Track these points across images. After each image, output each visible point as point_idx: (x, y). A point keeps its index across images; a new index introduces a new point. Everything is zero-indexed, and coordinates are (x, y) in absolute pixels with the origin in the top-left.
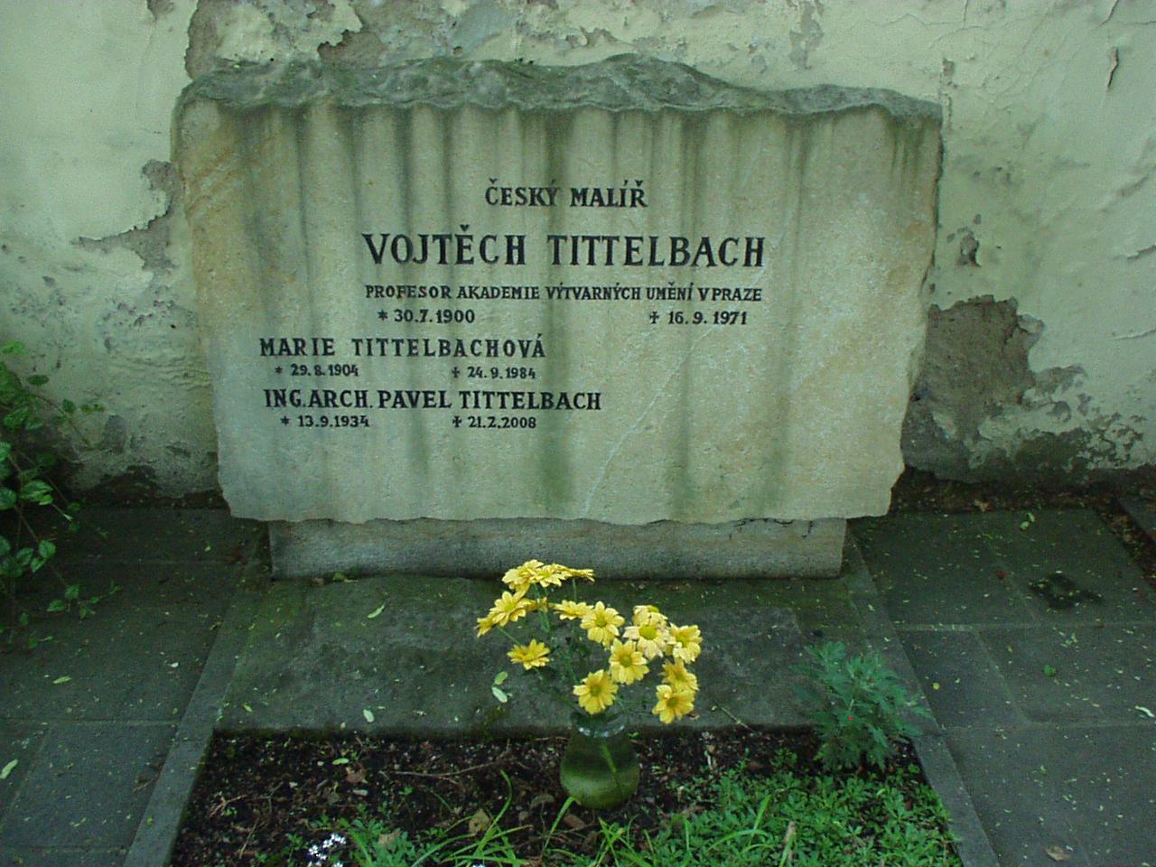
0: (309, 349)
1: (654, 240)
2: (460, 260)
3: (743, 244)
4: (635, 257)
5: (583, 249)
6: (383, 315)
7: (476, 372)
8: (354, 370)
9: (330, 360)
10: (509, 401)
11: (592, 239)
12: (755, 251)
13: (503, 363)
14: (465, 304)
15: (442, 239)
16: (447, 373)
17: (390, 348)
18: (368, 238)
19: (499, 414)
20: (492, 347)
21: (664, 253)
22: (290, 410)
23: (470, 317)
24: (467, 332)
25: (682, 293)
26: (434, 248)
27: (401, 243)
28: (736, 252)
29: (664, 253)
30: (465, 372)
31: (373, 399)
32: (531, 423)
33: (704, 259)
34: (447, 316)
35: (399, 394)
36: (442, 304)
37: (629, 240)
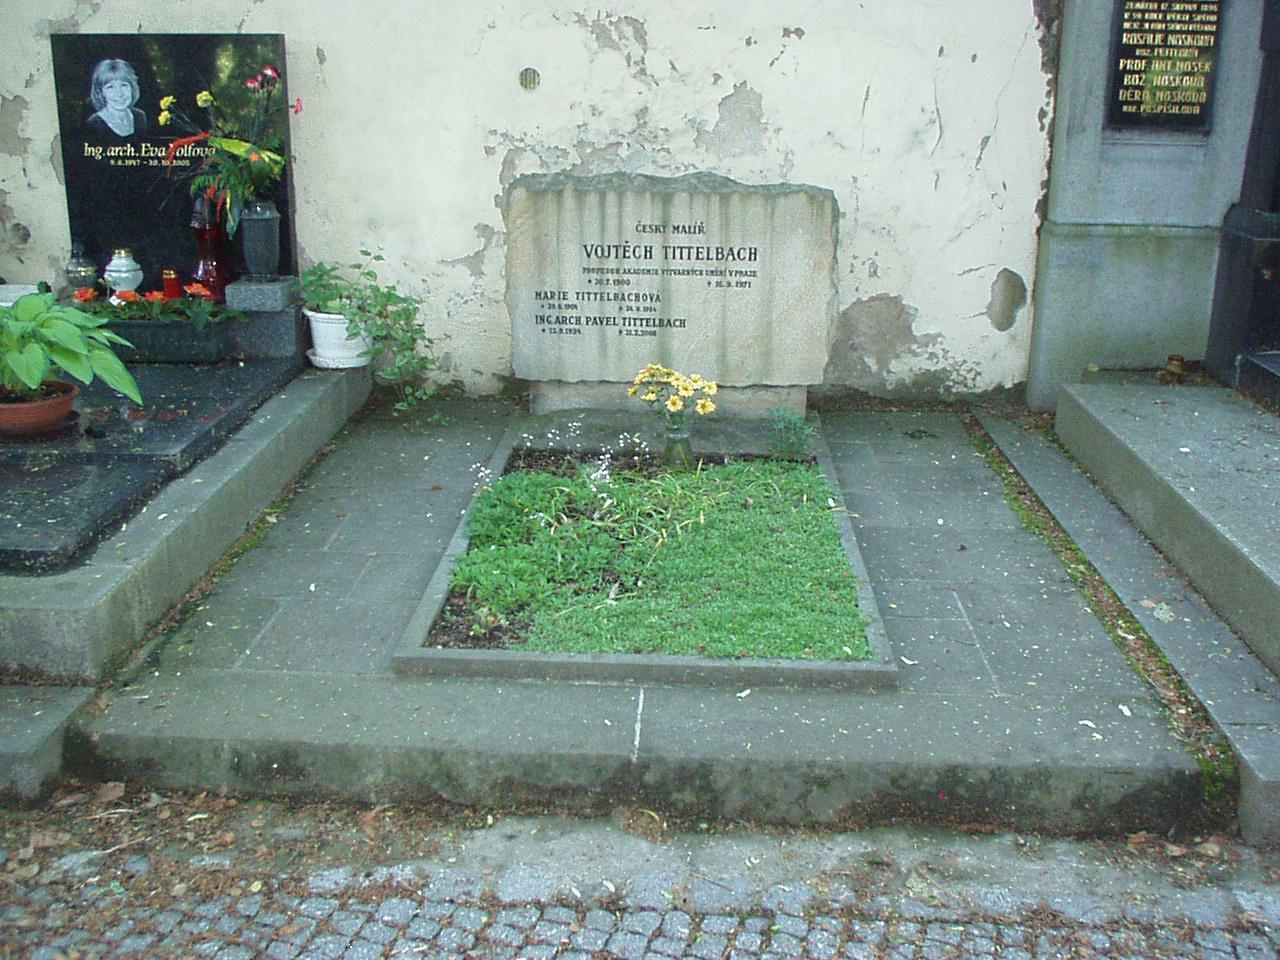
4: (701, 256)
5: (678, 252)
7: (630, 309)
8: (575, 306)
10: (644, 322)
11: (681, 248)
12: (753, 254)
13: (641, 304)
15: (616, 247)
16: (617, 309)
17: (592, 296)
18: (585, 247)
19: (640, 329)
21: (713, 254)
22: (546, 325)
23: (628, 282)
24: (626, 289)
26: (613, 251)
28: (745, 254)
29: (713, 254)
30: (625, 308)
31: (583, 320)
32: (654, 333)
33: (731, 257)
34: (618, 282)
36: (616, 276)
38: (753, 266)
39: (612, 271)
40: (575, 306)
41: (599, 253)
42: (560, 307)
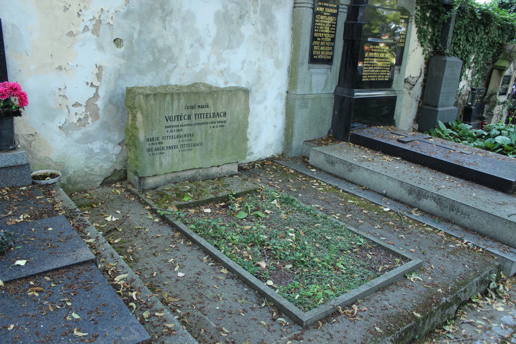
5: (200, 116)
7: (183, 141)
8: (162, 143)
9: (159, 141)
11: (201, 114)
12: (225, 114)
13: (186, 138)
14: (180, 128)
15: (178, 116)
17: (169, 138)
19: (186, 148)
20: (185, 135)
22: (151, 153)
23: (182, 130)
24: (181, 133)
26: (176, 117)
31: (165, 148)
32: (192, 150)
34: (178, 130)
38: (223, 119)
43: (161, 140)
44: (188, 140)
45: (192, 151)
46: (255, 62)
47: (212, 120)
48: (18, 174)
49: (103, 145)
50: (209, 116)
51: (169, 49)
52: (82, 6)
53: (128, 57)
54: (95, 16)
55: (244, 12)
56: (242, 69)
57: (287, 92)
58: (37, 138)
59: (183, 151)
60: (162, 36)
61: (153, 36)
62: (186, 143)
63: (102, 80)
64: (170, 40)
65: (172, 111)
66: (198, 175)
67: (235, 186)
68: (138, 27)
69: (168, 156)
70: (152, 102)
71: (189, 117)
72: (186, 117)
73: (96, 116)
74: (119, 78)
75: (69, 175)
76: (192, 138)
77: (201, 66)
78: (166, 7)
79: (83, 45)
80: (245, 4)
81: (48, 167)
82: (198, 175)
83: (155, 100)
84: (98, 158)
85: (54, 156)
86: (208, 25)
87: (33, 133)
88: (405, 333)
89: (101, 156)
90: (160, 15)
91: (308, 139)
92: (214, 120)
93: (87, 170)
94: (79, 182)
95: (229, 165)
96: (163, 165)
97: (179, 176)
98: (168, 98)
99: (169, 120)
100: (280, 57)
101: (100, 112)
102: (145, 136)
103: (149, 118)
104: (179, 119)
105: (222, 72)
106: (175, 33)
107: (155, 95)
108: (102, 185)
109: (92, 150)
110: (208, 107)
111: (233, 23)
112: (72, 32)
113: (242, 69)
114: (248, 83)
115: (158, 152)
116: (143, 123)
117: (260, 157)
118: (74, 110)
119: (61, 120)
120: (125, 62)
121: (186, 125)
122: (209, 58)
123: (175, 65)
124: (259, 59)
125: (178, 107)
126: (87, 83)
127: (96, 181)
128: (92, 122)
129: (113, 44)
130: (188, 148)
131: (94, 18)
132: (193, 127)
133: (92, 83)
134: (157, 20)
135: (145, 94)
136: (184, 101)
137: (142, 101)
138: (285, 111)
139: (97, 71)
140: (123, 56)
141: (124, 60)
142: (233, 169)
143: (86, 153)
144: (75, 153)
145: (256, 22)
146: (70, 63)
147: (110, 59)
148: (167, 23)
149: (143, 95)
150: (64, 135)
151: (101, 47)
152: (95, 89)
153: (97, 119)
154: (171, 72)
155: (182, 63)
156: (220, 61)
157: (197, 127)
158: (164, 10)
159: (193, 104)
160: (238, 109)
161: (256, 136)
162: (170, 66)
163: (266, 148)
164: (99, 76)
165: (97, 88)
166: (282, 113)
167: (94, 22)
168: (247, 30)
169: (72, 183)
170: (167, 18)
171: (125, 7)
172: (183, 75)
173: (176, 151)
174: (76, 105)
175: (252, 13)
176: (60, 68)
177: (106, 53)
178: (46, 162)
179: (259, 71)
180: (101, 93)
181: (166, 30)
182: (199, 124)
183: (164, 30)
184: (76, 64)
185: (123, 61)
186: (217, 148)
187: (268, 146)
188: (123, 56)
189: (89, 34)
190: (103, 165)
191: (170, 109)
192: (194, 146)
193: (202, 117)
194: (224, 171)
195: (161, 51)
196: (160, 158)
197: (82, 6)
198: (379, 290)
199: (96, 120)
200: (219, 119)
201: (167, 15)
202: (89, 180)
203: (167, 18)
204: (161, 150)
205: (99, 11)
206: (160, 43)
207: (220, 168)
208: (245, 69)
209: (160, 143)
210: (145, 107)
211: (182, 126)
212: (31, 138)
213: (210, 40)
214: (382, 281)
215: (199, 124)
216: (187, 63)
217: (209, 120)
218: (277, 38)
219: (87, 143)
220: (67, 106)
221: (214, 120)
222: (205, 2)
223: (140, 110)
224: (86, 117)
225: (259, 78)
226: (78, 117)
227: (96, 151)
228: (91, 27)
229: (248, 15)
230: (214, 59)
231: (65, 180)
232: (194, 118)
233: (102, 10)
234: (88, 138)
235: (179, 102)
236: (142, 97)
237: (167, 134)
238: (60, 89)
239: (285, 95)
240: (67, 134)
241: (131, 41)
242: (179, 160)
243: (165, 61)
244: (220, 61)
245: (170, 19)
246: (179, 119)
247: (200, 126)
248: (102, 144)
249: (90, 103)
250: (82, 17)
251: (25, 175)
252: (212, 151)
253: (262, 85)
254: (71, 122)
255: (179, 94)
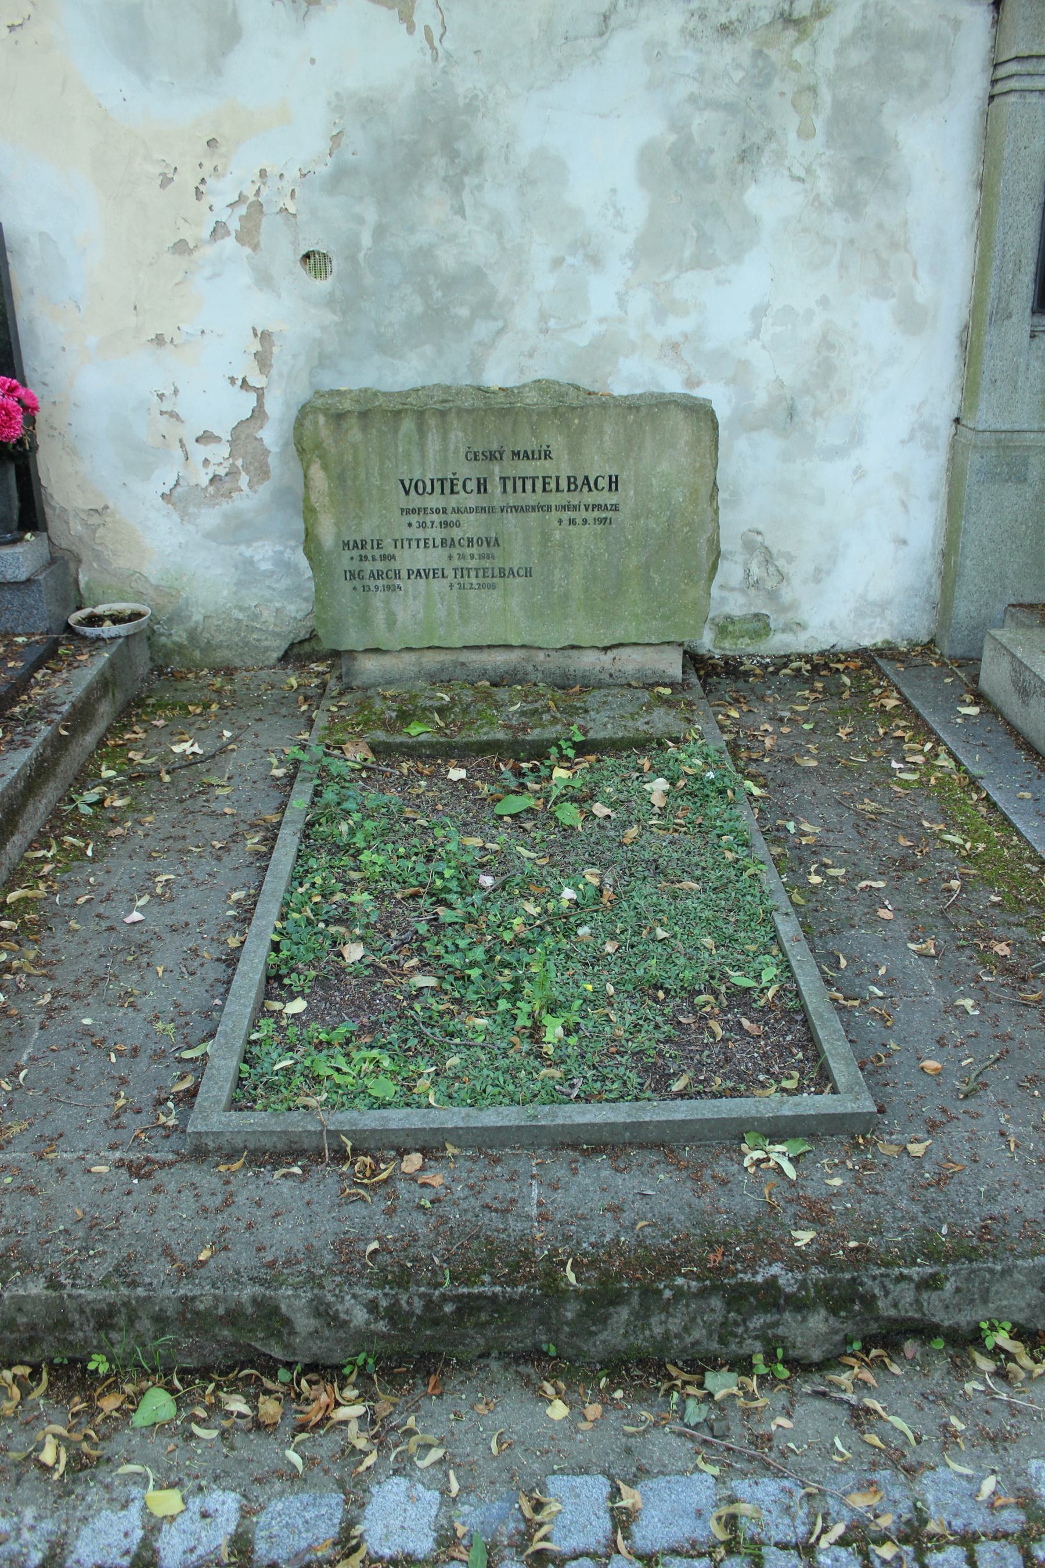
0: (369, 546)
1: (558, 478)
2: (452, 492)
3: (607, 479)
5: (519, 483)
6: (410, 525)
8: (393, 557)
9: (382, 552)
10: (481, 573)
11: (524, 479)
12: (614, 483)
13: (474, 550)
14: (453, 517)
16: (446, 557)
17: (414, 544)
18: (402, 482)
19: (474, 581)
20: (470, 541)
21: (564, 484)
22: (357, 583)
23: (458, 524)
25: (575, 507)
27: (420, 484)
28: (603, 483)
29: (564, 484)
30: (456, 557)
31: (404, 574)
32: (494, 586)
33: (586, 488)
34: (445, 524)
35: (419, 571)
36: (443, 517)
37: (544, 478)
38: (611, 499)
39: (437, 511)
40: (393, 557)
41: (421, 491)
42: (374, 559)
43: (390, 550)
44: (481, 557)
45: (494, 592)
46: (810, 314)
47: (564, 498)
48: (16, 603)
49: (282, 553)
50: (553, 486)
51: (478, 275)
52: (208, 166)
53: (346, 305)
54: (245, 193)
55: (757, 138)
56: (756, 334)
57: (957, 421)
58: (108, 519)
59: (462, 587)
60: (452, 238)
61: (421, 238)
62: (472, 564)
63: (274, 371)
64: (480, 247)
65: (423, 464)
66: (530, 668)
67: (602, 717)
68: (371, 215)
69: (415, 598)
70: (355, 435)
71: (482, 486)
72: (472, 485)
73: (262, 472)
74: (321, 365)
75: (192, 624)
76: (495, 551)
77: (593, 328)
78: (461, 146)
79: (215, 276)
80: (760, 107)
81: (139, 596)
82: (530, 668)
83: (364, 429)
84: (269, 587)
85: (152, 570)
86: (614, 191)
87: (100, 507)
88: (459, 1311)
89: (277, 581)
90: (442, 173)
91: (1027, 599)
92: (574, 499)
93: (241, 616)
94: (220, 646)
95: (648, 649)
96: (399, 624)
97: (463, 664)
98: (408, 425)
99: (413, 492)
100: (924, 291)
101: (272, 461)
102: (338, 535)
103: (349, 483)
104: (447, 490)
105: (675, 346)
106: (496, 225)
107: (364, 415)
108: (285, 658)
109: (250, 562)
110: (547, 455)
111: (711, 178)
112: (183, 242)
113: (756, 334)
114: (782, 385)
115: (380, 583)
116: (331, 495)
117: (833, 640)
118: (199, 452)
119: (165, 477)
120: (336, 319)
121: (471, 510)
122: (622, 300)
123: (500, 324)
124: (824, 302)
125: (441, 453)
126: (232, 380)
127: (267, 649)
128: (250, 485)
129: (299, 268)
130: (481, 580)
131: (242, 199)
132: (498, 515)
133: (244, 381)
134: (432, 189)
135: (333, 411)
136: (460, 434)
137: (324, 432)
138: (944, 490)
139: (256, 346)
140: (330, 301)
141: (334, 312)
142: (661, 666)
143: (236, 568)
144: (208, 568)
145: (808, 170)
146: (185, 328)
147: (294, 310)
148: (466, 195)
149: (326, 415)
150: (176, 517)
151: (264, 280)
152: (253, 396)
153: (264, 479)
154: (488, 346)
155: (524, 317)
156: (661, 312)
157: (511, 517)
158: (453, 155)
159: (495, 447)
160: (664, 467)
161: (818, 570)
162: (483, 329)
163: (860, 613)
164: (263, 360)
165: (260, 393)
166: (933, 497)
167: (243, 210)
168: (771, 199)
169: (203, 645)
170: (467, 180)
171: (329, 159)
172: (531, 356)
173: (438, 585)
174: (206, 438)
175: (792, 136)
176: (159, 340)
177: (279, 296)
178: (134, 584)
179: (826, 343)
180: (274, 406)
181: (464, 217)
182: (516, 509)
183: (458, 218)
184: (200, 328)
185: (331, 317)
186: (586, 590)
187: (865, 609)
188: (330, 301)
189: (229, 243)
190: (284, 607)
191: (416, 456)
192: (502, 573)
193: (519, 488)
194: (630, 668)
195: (451, 283)
196: (387, 602)
197: (208, 166)
198: (575, 1146)
199: (259, 483)
200: (590, 498)
201: (465, 171)
202: (247, 644)
203: (467, 180)
204: (390, 580)
205: (256, 177)
206: (447, 259)
207: (611, 654)
208: (765, 336)
209: (384, 557)
210: (333, 451)
211: (457, 511)
212: (95, 520)
213: (626, 242)
214: (598, 1120)
215: (516, 509)
216: (543, 317)
217: (555, 499)
218: (905, 223)
219: (236, 543)
220: (181, 441)
221: (574, 499)
222: (603, 116)
223: (320, 457)
224: (233, 473)
225: (826, 371)
226: (211, 471)
227: (265, 566)
228: (234, 225)
229: (773, 146)
230: (640, 302)
231: (184, 635)
232: (499, 489)
233: (263, 173)
234: (237, 530)
235: (445, 438)
236: (322, 420)
237: (407, 533)
238: (161, 396)
239: (946, 430)
240: (184, 515)
241: (352, 259)
242: (449, 614)
243: (464, 312)
244: (661, 312)
245: (476, 181)
246: (447, 490)
247: (521, 515)
248: (278, 548)
249: (243, 434)
250: (208, 199)
251: (33, 607)
252: (566, 597)
253: (842, 392)
254: (193, 482)
255: (443, 414)
